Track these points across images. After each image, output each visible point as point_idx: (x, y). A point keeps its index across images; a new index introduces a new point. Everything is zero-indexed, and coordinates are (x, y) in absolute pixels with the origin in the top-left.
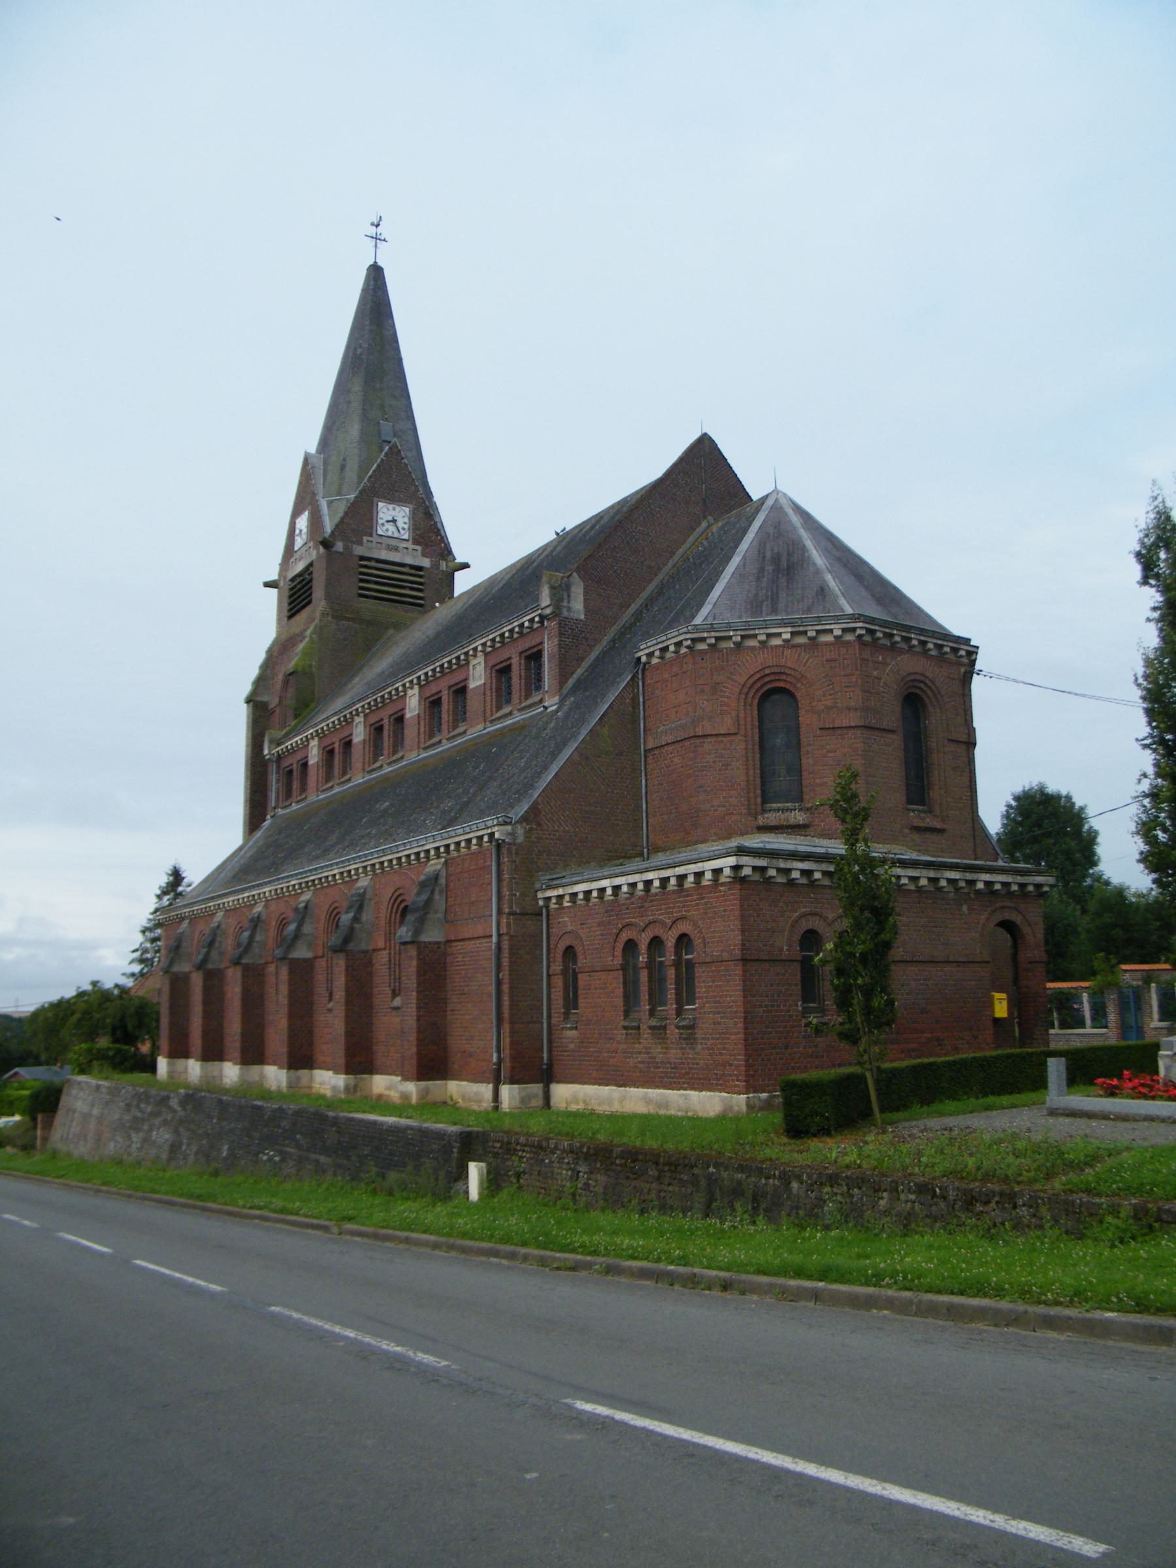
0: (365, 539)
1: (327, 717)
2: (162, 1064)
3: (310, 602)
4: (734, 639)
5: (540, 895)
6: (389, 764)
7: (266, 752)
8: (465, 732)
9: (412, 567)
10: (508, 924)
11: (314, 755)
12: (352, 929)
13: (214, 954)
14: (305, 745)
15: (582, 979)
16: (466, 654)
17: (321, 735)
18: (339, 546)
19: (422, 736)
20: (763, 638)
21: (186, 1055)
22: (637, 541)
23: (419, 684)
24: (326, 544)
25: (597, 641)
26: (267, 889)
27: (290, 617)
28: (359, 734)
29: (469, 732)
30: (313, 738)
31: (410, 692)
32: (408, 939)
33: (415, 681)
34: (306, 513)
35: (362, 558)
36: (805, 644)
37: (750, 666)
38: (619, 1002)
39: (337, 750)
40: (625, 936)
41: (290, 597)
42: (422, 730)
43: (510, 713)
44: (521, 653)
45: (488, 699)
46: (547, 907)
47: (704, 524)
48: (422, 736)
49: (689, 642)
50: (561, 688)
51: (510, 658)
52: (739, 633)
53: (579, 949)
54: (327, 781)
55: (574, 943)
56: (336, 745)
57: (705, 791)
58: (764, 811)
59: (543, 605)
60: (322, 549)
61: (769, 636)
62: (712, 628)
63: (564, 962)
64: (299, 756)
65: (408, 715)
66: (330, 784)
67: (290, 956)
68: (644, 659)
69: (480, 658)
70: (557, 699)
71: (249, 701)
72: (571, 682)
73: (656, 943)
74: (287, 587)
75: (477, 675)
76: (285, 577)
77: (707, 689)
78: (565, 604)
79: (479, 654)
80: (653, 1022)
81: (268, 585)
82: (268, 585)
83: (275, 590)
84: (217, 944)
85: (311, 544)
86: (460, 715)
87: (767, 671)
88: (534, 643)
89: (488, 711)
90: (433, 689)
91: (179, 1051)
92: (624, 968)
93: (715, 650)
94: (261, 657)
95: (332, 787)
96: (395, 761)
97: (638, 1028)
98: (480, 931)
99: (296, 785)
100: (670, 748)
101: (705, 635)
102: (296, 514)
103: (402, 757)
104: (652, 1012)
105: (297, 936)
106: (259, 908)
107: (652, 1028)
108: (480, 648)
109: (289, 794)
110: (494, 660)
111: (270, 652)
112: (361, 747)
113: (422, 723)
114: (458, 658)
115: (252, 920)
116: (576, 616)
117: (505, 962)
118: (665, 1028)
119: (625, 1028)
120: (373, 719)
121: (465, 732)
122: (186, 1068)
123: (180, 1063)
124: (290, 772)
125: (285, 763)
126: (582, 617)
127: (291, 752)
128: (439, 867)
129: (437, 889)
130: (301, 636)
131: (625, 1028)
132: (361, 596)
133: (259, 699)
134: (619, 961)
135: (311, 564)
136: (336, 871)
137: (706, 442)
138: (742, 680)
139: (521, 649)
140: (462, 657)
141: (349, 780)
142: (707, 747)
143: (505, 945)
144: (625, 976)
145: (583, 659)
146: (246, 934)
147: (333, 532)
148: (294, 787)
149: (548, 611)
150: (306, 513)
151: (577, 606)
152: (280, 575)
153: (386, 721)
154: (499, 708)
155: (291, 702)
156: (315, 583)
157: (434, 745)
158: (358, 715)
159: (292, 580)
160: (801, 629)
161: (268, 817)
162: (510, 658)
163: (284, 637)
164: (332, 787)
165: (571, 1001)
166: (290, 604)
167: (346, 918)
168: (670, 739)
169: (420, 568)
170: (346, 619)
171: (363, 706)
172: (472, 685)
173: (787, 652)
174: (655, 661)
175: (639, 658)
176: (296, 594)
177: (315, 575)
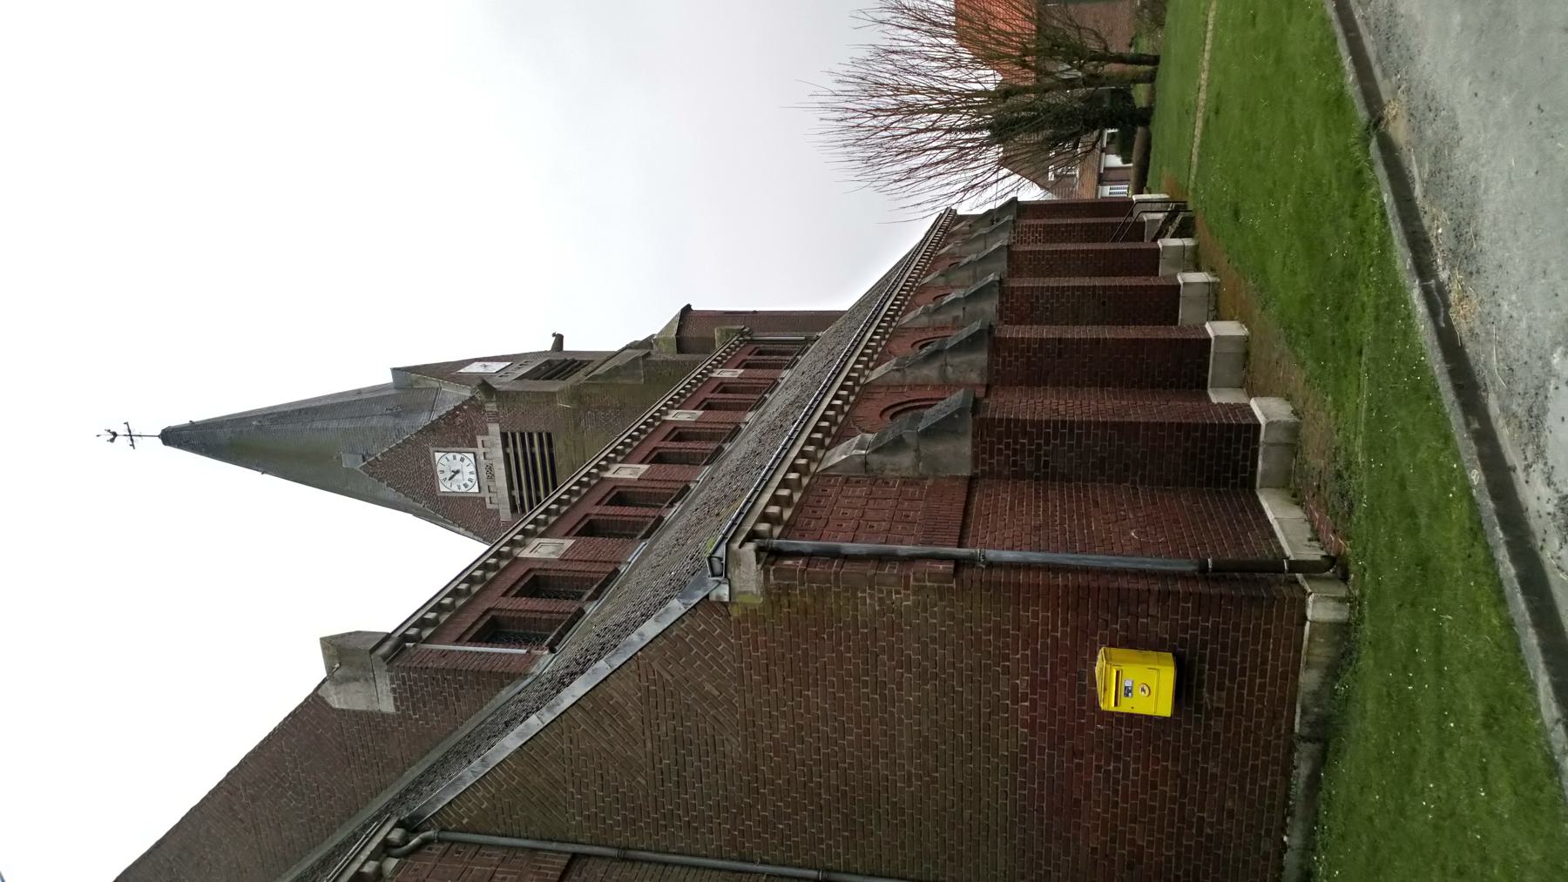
0: (489, 506)
9: (505, 445)
169: (504, 436)
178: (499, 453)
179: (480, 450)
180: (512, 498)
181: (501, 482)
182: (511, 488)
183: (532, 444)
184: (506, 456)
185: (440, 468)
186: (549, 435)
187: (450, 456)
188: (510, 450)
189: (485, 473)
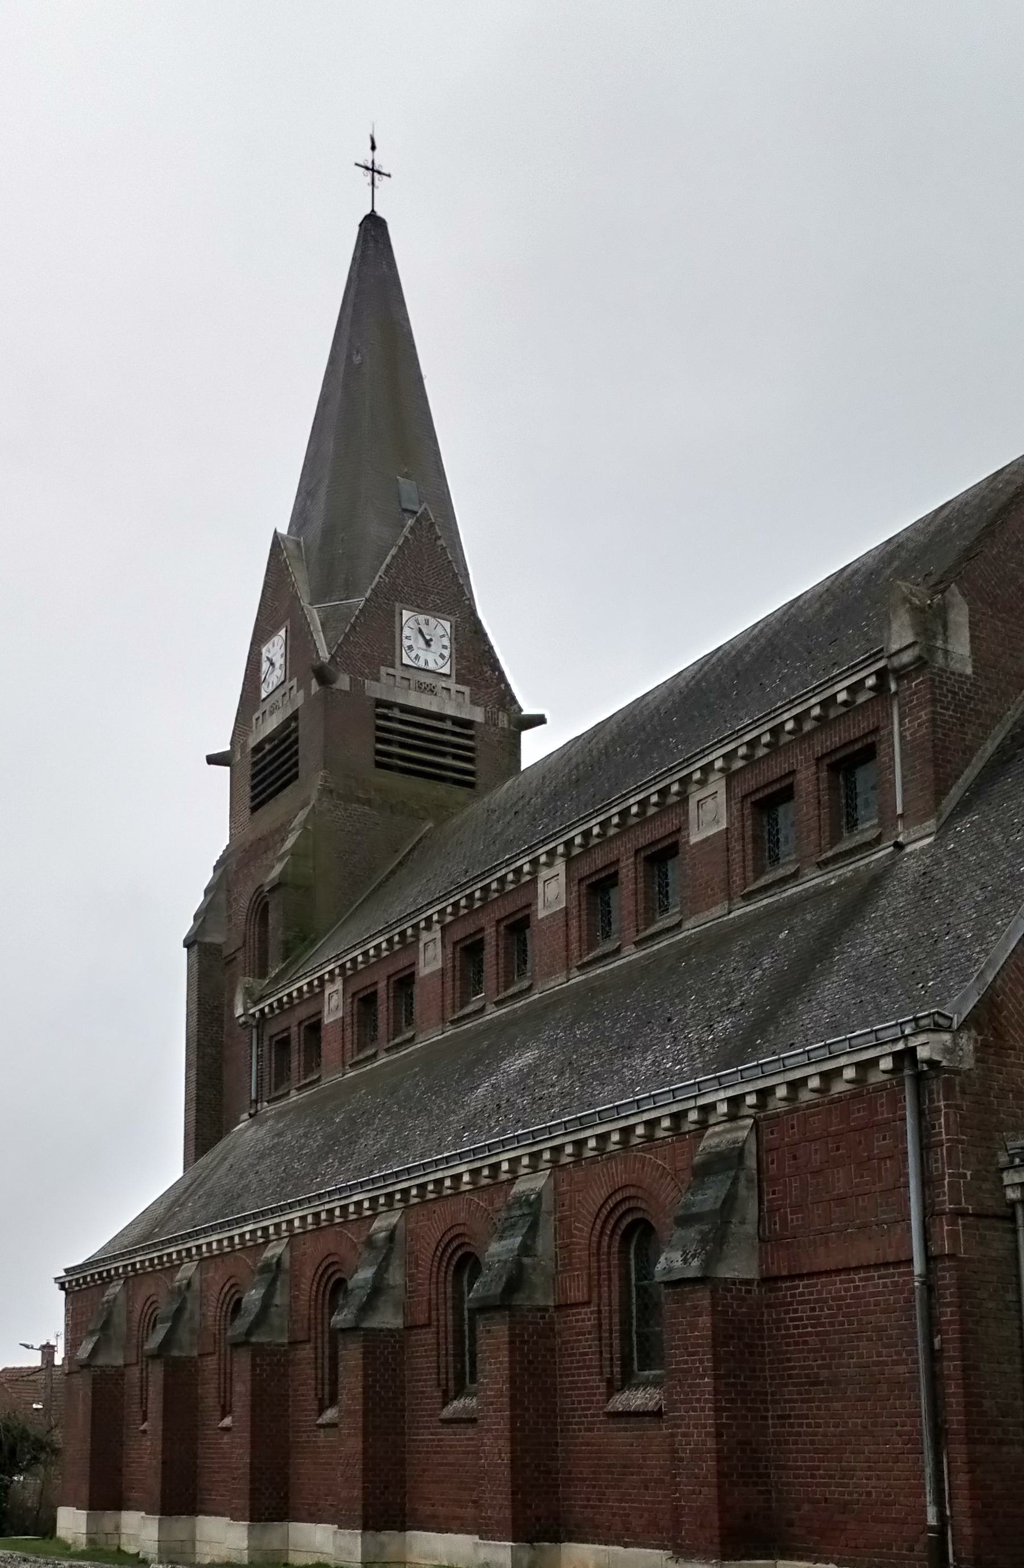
2: (72, 1522)
3: (296, 776)
6: (499, 1004)
7: (239, 1011)
8: (679, 925)
11: (334, 1007)
12: (519, 1266)
13: (184, 1335)
14: (316, 992)
16: (685, 781)
18: (343, 682)
19: (574, 946)
21: (119, 1504)
23: (567, 855)
24: (323, 676)
26: (295, 1215)
27: (254, 809)
28: (431, 958)
29: (687, 925)
30: (332, 980)
31: (544, 873)
32: (691, 1274)
33: (561, 849)
34: (282, 633)
35: (380, 703)
41: (254, 776)
42: (574, 934)
43: (795, 876)
44: (819, 760)
45: (736, 857)
48: (574, 946)
50: (938, 803)
51: (792, 773)
54: (361, 1047)
56: (382, 985)
59: (895, 647)
60: (315, 686)
64: (302, 1012)
66: (370, 1052)
67: (365, 1325)
69: (717, 784)
70: (931, 825)
71: (188, 944)
72: (956, 793)
74: (249, 759)
75: (707, 817)
76: (244, 746)
79: (713, 777)
81: (212, 760)
82: (212, 760)
83: (228, 768)
84: (186, 1315)
85: (294, 682)
86: (656, 899)
88: (855, 733)
89: (737, 880)
90: (599, 859)
91: (106, 1497)
94: (207, 876)
95: (375, 1056)
96: (514, 997)
99: (296, 1061)
102: (260, 636)
103: (530, 989)
105: (377, 1289)
106: (275, 1250)
113: (574, 923)
114: (663, 793)
115: (266, 1268)
116: (956, 666)
120: (459, 933)
121: (679, 925)
122: (117, 1527)
123: (108, 1519)
124: (283, 1044)
125: (272, 1029)
130: (281, 831)
133: (208, 940)
135: (294, 717)
139: (819, 750)
141: (411, 1041)
145: (970, 751)
146: (253, 1296)
147: (333, 657)
148: (294, 1064)
149: (906, 658)
150: (282, 633)
152: (232, 743)
154: (759, 873)
156: (302, 746)
157: (605, 956)
158: (428, 928)
159: (257, 749)
162: (792, 773)
163: (251, 838)
166: (253, 788)
167: (499, 1250)
170: (358, 800)
171: (442, 912)
176: (263, 768)
183: (456, 757)
184: (442, 717)
188: (448, 725)
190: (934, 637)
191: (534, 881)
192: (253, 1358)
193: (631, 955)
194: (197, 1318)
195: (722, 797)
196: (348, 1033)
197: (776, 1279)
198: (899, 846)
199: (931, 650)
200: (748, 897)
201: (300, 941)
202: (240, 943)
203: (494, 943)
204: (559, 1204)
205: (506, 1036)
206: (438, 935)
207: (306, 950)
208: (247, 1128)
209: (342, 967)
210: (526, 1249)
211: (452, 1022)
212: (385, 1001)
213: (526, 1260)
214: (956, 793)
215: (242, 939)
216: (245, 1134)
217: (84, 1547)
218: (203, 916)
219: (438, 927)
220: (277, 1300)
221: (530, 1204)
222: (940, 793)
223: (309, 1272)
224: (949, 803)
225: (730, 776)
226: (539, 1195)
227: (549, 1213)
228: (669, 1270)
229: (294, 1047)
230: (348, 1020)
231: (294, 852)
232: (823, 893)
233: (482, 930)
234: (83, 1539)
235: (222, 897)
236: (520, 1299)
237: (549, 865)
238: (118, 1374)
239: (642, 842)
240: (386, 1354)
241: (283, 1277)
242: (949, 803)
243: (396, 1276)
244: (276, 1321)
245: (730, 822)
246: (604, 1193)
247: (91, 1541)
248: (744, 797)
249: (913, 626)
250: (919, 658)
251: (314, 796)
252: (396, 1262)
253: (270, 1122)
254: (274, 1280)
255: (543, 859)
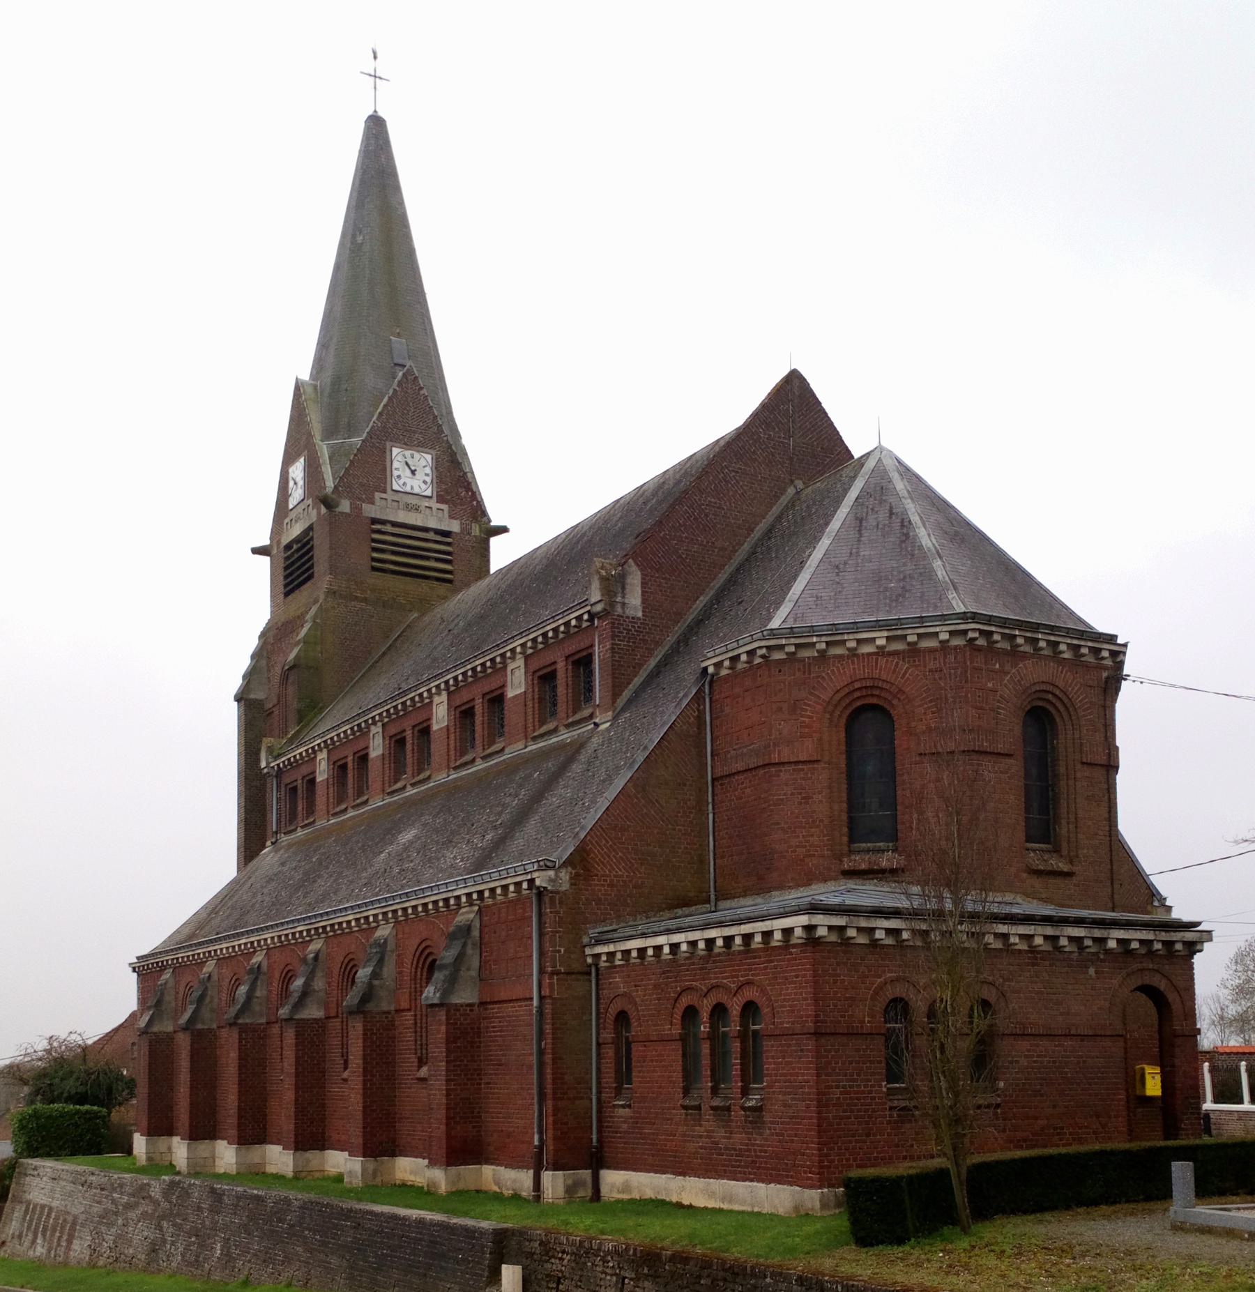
1: (333, 724)
2: (140, 1143)
4: (818, 647)
5: (588, 951)
6: (413, 785)
8: (502, 750)
10: (551, 985)
14: (311, 757)
15: (637, 1050)
16: (503, 655)
17: (331, 747)
19: (452, 753)
20: (852, 644)
22: (706, 515)
23: (447, 689)
25: (658, 644)
28: (377, 747)
29: (507, 751)
30: (321, 750)
31: (436, 699)
32: (436, 1001)
33: (443, 686)
36: (904, 651)
37: (835, 681)
38: (678, 1076)
39: (350, 765)
40: (684, 1001)
43: (554, 731)
44: (567, 657)
45: (530, 711)
46: (596, 965)
47: (791, 491)
48: (452, 753)
49: (764, 651)
50: (614, 701)
51: (555, 663)
52: (824, 639)
53: (632, 1014)
54: (339, 803)
55: (628, 1007)
56: (350, 758)
57: (782, 829)
58: (851, 852)
59: (593, 600)
61: (859, 641)
62: (791, 632)
63: (615, 1028)
64: (305, 770)
65: (435, 727)
66: (343, 806)
68: (711, 670)
69: (520, 662)
71: (239, 698)
72: (627, 694)
73: (719, 1011)
75: (516, 681)
77: (785, 706)
78: (619, 599)
79: (519, 656)
80: (717, 1102)
86: (497, 728)
87: (857, 685)
88: (583, 646)
90: (465, 696)
91: (160, 1127)
92: (683, 1039)
93: (797, 661)
94: (253, 643)
95: (346, 809)
96: (420, 782)
97: (699, 1108)
98: (518, 992)
100: (741, 777)
101: (784, 642)
103: (429, 778)
104: (715, 1091)
107: (713, 1108)
108: (519, 649)
109: (293, 816)
110: (535, 665)
111: (263, 635)
112: (379, 763)
113: (452, 737)
114: (493, 660)
116: (630, 612)
117: (548, 1028)
118: (728, 1109)
119: (685, 1107)
120: (393, 730)
121: (502, 750)
122: (170, 1149)
124: (294, 789)
126: (640, 614)
127: (294, 765)
128: (472, 916)
129: (469, 942)
131: (685, 1107)
132: (374, 569)
133: (252, 696)
134: (677, 1031)
136: (350, 918)
137: (796, 382)
138: (825, 696)
139: (567, 652)
140: (498, 659)
141: (366, 802)
142: (784, 777)
143: (548, 1009)
144: (684, 1048)
145: (640, 666)
148: (300, 808)
149: (599, 608)
151: (634, 601)
153: (409, 733)
154: (542, 723)
155: (294, 705)
157: (466, 764)
158: (374, 723)
160: (899, 633)
161: (268, 843)
162: (555, 663)
164: (346, 809)
165: (624, 1073)
168: (740, 766)
172: (510, 693)
173: (882, 661)
174: (724, 672)
175: (706, 669)
177: (316, 542)
178: (432, 524)
179: (434, 504)
180: (384, 522)
181: (403, 517)
182: (394, 524)
185: (417, 455)
186: (450, 581)
187: (428, 470)
189: (410, 501)
190: (615, 596)
191: (431, 702)
192: (240, 1035)
193: (480, 766)
194: (216, 1000)
195: (523, 670)
196: (331, 790)
197: (486, 1003)
198: (596, 725)
199: (612, 604)
200: (535, 739)
201: (310, 709)
202: (275, 701)
203: (409, 744)
204: (397, 946)
205: (409, 811)
206: (380, 730)
207: (315, 716)
208: (270, 852)
209: (325, 742)
210: (375, 975)
211: (389, 794)
212: (351, 770)
213: (376, 982)
214: (627, 694)
215: (273, 703)
216: (268, 857)
217: (144, 1163)
218: (249, 676)
219: (380, 724)
220: (258, 994)
221: (379, 945)
222: (615, 695)
223: (277, 975)
224: (621, 701)
225: (527, 658)
226: (386, 941)
227: (392, 951)
228: (427, 998)
229: (300, 795)
230: (331, 781)
231: (305, 641)
232: (562, 746)
233: (404, 731)
234: (144, 1157)
235: (264, 663)
236: (370, 1006)
237: (439, 694)
238: (169, 1038)
239: (487, 689)
240: (311, 1039)
241: (262, 977)
242: (621, 701)
243: (319, 984)
244: (257, 1008)
245: (527, 689)
246: (418, 941)
247: (149, 1159)
248: (534, 672)
249: (601, 590)
250: (605, 610)
251: (322, 597)
252: (319, 974)
253: (282, 851)
254: (256, 979)
255: (434, 690)
